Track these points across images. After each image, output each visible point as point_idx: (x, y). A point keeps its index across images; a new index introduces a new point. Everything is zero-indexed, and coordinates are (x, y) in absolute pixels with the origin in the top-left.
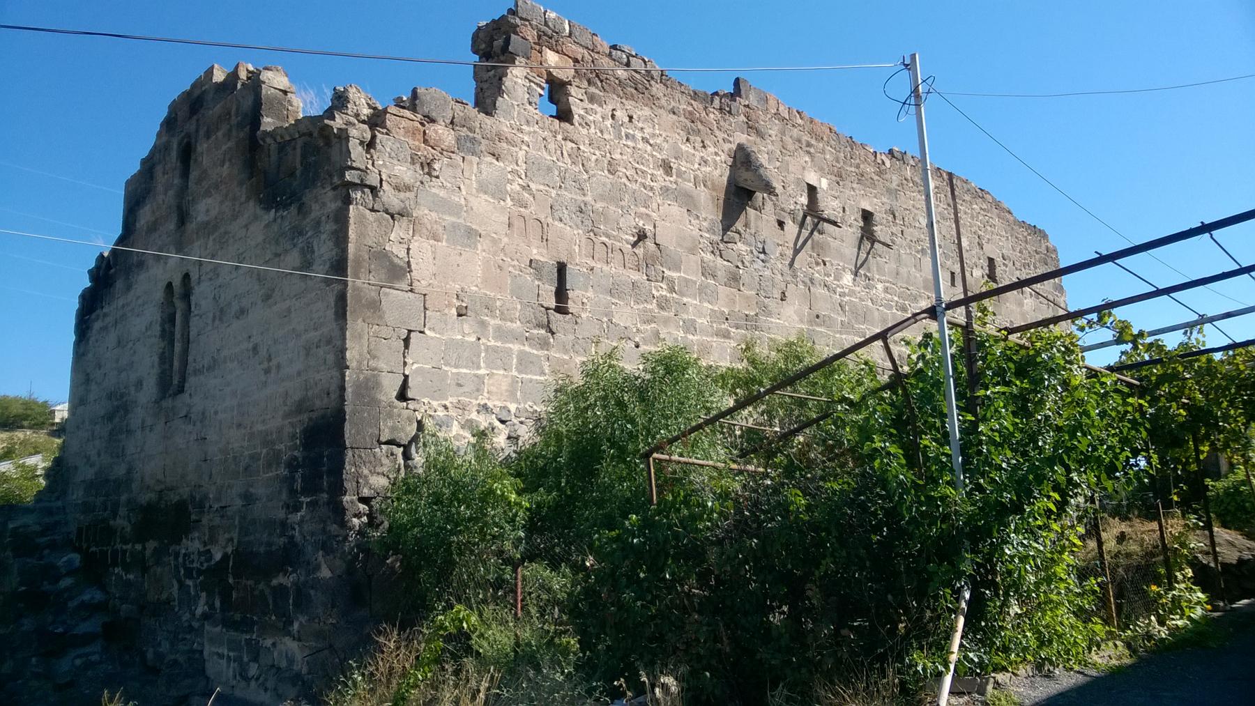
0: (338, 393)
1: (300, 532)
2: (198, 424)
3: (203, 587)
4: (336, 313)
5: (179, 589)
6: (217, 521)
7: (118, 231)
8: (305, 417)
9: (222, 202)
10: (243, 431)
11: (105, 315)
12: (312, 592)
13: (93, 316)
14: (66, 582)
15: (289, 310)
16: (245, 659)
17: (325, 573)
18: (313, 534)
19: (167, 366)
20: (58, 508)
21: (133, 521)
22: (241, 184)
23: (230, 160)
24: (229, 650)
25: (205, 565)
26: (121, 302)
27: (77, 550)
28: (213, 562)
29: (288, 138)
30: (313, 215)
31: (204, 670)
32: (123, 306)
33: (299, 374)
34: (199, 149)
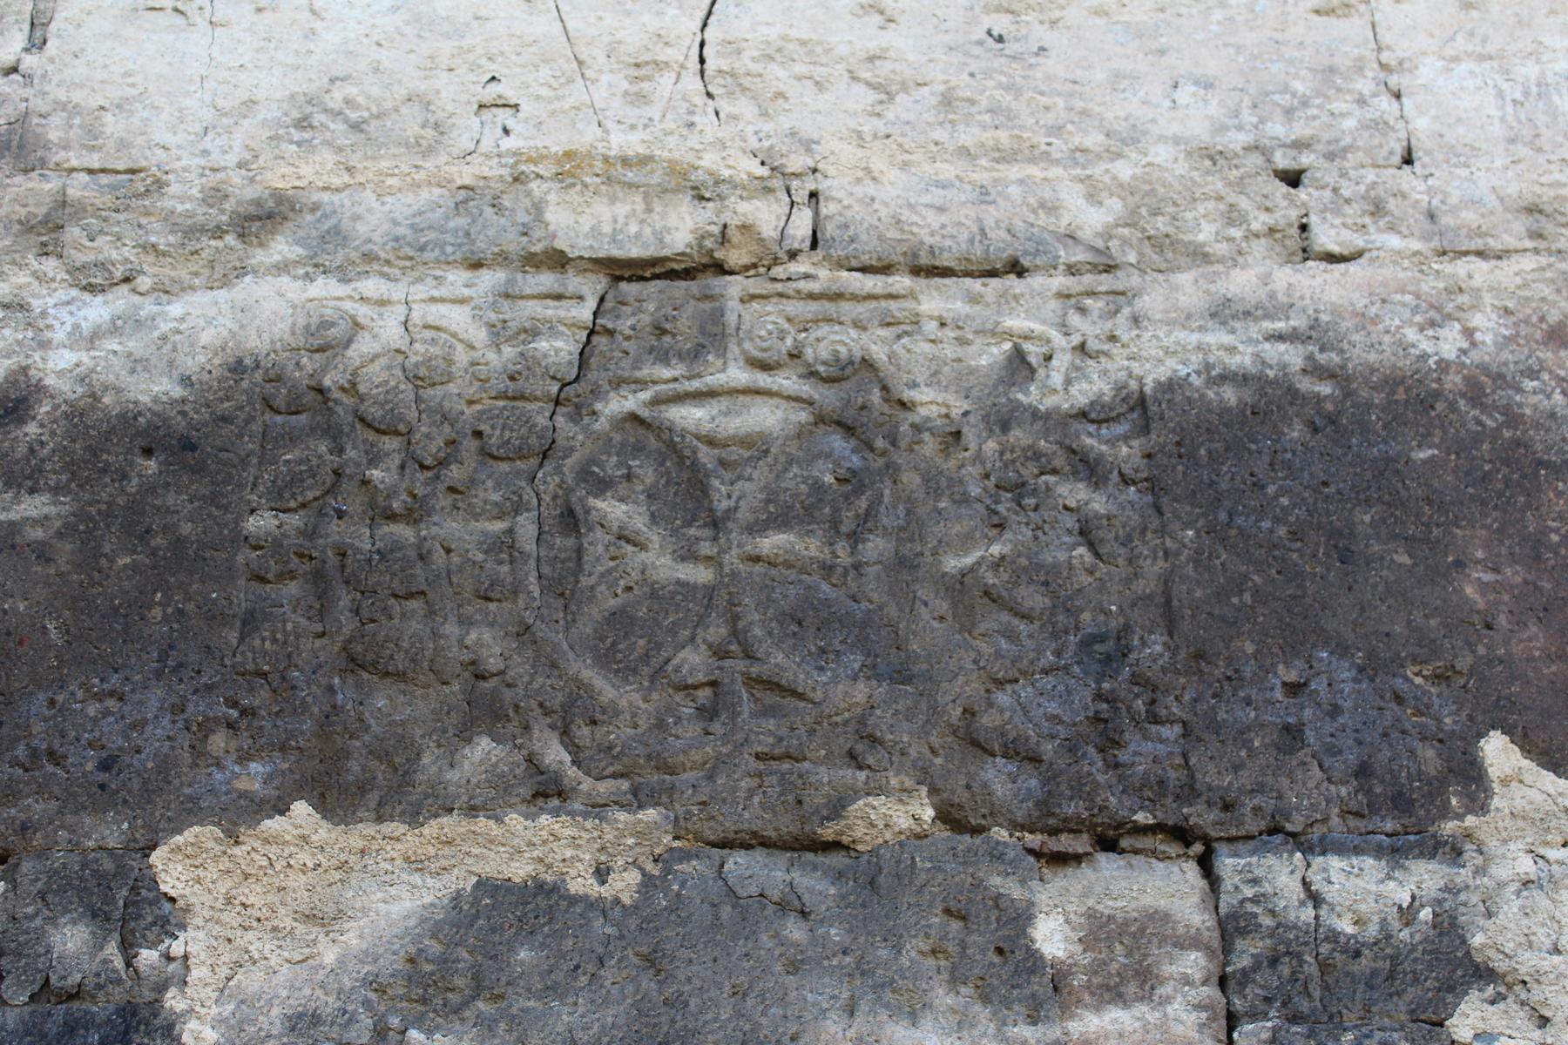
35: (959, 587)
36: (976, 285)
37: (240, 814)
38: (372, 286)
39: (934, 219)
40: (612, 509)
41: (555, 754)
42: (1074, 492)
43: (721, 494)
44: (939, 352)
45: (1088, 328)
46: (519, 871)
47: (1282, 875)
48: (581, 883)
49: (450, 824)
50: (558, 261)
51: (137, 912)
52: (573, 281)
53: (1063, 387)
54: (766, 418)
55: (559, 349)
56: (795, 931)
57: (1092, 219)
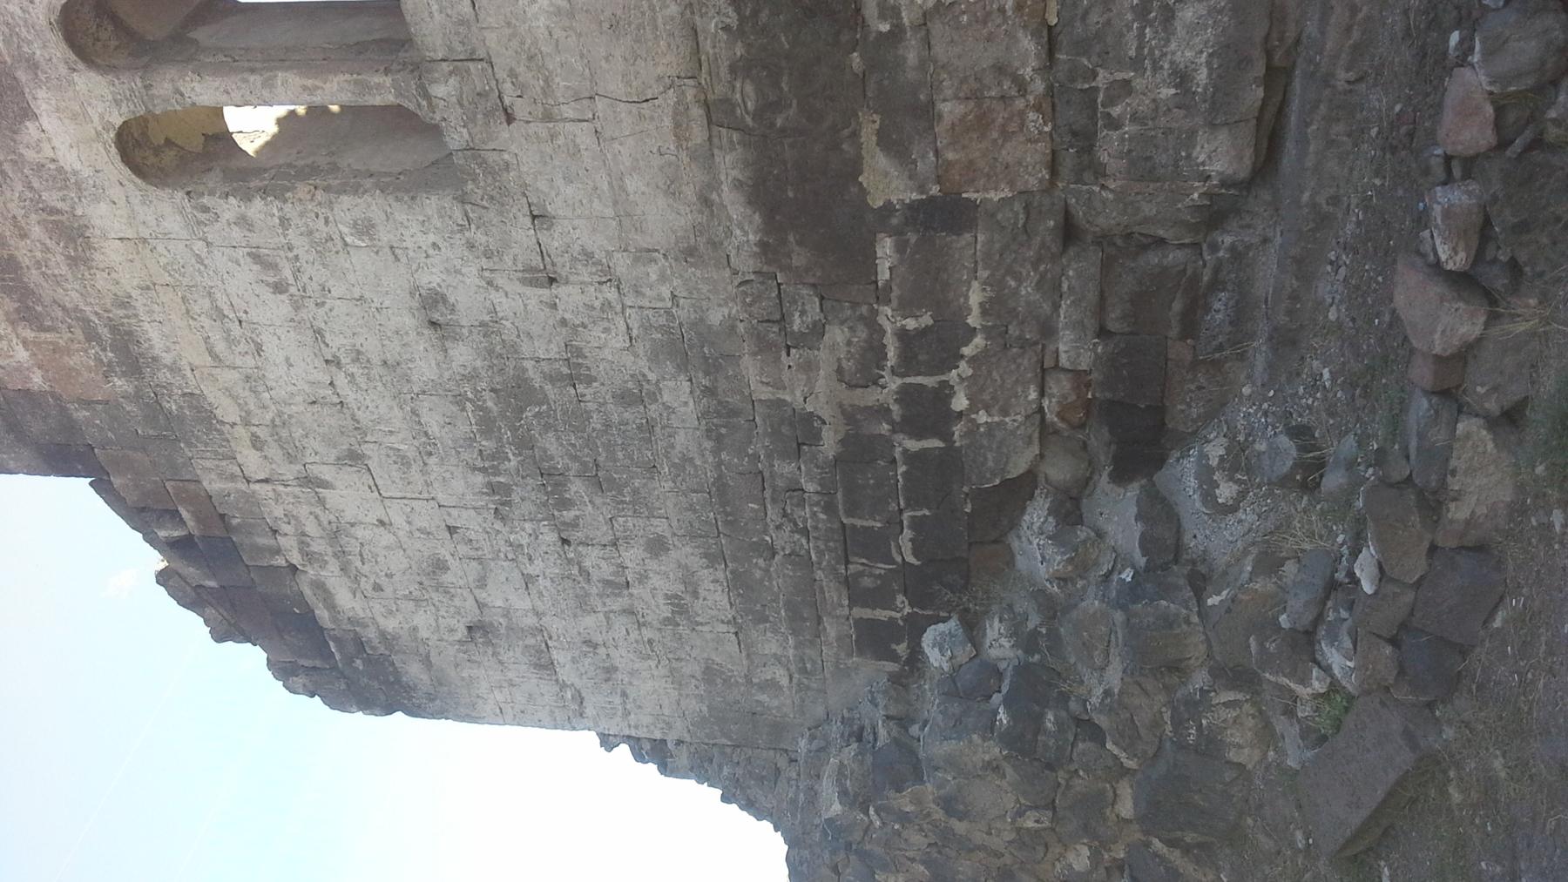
7: (81, 486)
11: (309, 556)
13: (322, 614)
14: (999, 643)
19: (368, 183)
20: (813, 738)
21: (814, 311)
26: (251, 461)
27: (916, 658)
32: (257, 443)
36: (701, 39)
37: (863, 191)
38: (723, 178)
39: (682, 48)
40: (779, 122)
41: (846, 132)
42: (764, 16)
43: (772, 98)
45: (712, 12)
46: (874, 138)
48: (877, 126)
49: (864, 153)
50: (710, 138)
51: (888, 208)
52: (715, 133)
53: (732, 19)
54: (749, 88)
55: (735, 136)
56: (886, 82)
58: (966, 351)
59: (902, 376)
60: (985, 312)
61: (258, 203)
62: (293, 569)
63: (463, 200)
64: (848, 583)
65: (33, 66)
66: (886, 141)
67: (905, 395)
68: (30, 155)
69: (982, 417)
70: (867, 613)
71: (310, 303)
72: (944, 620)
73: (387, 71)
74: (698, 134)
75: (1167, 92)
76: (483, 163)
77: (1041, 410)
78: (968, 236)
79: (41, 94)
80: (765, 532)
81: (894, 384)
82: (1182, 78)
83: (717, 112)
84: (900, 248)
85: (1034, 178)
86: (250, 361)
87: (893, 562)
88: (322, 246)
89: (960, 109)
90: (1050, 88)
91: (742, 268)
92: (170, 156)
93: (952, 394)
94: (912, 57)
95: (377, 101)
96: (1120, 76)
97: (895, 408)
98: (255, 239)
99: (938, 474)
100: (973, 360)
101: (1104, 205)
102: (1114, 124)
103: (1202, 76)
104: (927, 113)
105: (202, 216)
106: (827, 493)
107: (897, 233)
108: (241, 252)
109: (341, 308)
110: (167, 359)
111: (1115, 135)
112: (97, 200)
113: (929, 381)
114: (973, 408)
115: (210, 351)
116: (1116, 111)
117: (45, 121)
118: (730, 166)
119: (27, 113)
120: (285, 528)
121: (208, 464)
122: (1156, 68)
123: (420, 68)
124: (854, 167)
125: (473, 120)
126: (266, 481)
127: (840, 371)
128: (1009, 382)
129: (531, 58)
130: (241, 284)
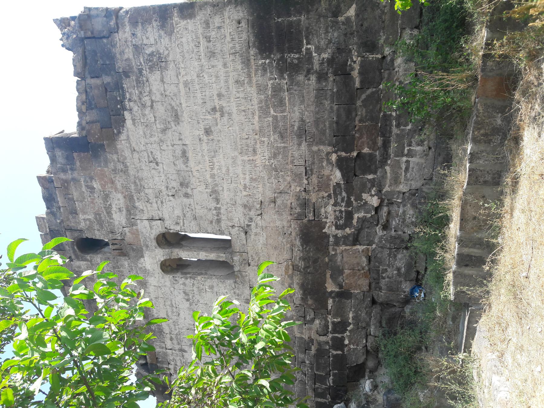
0: (239, 8)
1: (324, 50)
2: (252, 213)
3: (359, 198)
4: (191, 16)
5: (360, 245)
6: (314, 179)
8: (252, 51)
9: (116, 190)
10: (258, 146)
12: (366, 24)
15: (186, 84)
16: (409, 127)
17: (352, 12)
18: (327, 32)
21: (312, 315)
22: (106, 162)
23: (92, 178)
24: (403, 155)
25: (344, 194)
26: (169, 344)
28: (342, 182)
29: (84, 97)
30: (131, 57)
31: (417, 190)
32: (171, 339)
33: (225, 65)
34: (82, 226)
35: (313, 255)
37: (326, 288)
42: (307, 249)
44: (298, 254)
47: (331, 243)
51: (332, 292)
53: (301, 248)
54: (303, 263)
55: (298, 273)
57: (289, 245)
58: (348, 328)
59: (332, 334)
60: (353, 319)
61: (189, 280)
62: (171, 374)
63: (235, 282)
64: (315, 390)
65: (147, 246)
66: (331, 276)
67: (333, 339)
68: (140, 266)
69: (352, 347)
70: (319, 400)
71: (194, 304)
72: (340, 403)
73: (224, 253)
74: (290, 272)
75: (395, 272)
76: (241, 275)
77: (366, 346)
78: (350, 301)
79: (147, 252)
80: (295, 374)
81: (330, 336)
82: (399, 269)
83: (295, 268)
84: (334, 302)
85: (366, 288)
86: (176, 318)
87: (327, 385)
88: (200, 291)
89: (349, 271)
90: (369, 270)
91: (297, 303)
92: (169, 268)
93: (344, 340)
94: (339, 260)
95: (221, 260)
96: (385, 268)
97: (330, 342)
98: (186, 288)
99: (340, 361)
100: (350, 331)
101: (382, 295)
102: (384, 278)
103: (403, 269)
104: (341, 272)
105: (175, 282)
106: (311, 364)
107: (333, 298)
108: (181, 291)
109: (201, 306)
110: (156, 316)
111: (384, 280)
112: (152, 276)
113: (339, 336)
114: (349, 344)
115: (167, 315)
116: (384, 275)
117: (146, 258)
118: (297, 279)
119: (142, 256)
120: (172, 363)
121: (158, 344)
122: (393, 267)
123: (232, 253)
124: (325, 282)
125: (241, 265)
126: (171, 349)
127: (317, 331)
128: (359, 337)
129: (256, 253)
130: (179, 298)
